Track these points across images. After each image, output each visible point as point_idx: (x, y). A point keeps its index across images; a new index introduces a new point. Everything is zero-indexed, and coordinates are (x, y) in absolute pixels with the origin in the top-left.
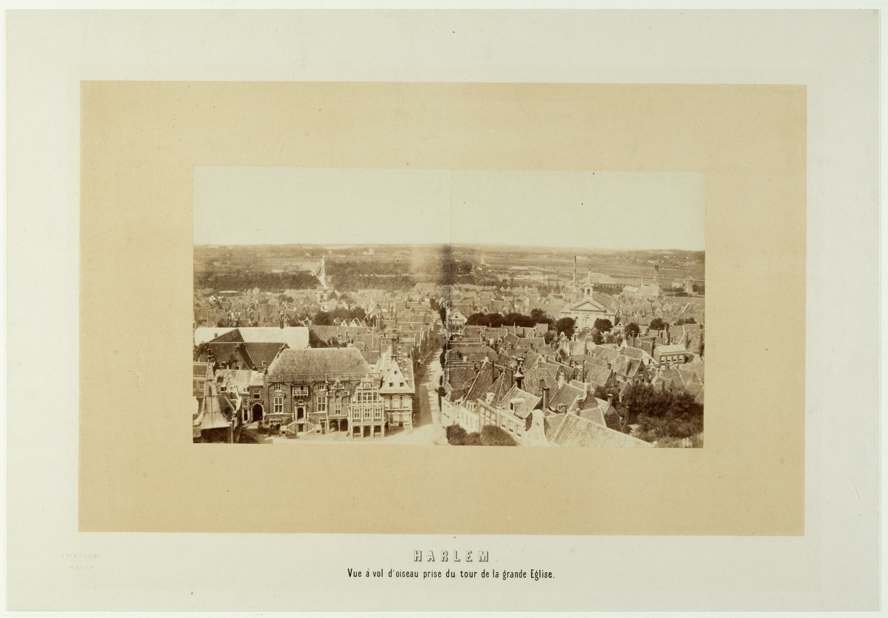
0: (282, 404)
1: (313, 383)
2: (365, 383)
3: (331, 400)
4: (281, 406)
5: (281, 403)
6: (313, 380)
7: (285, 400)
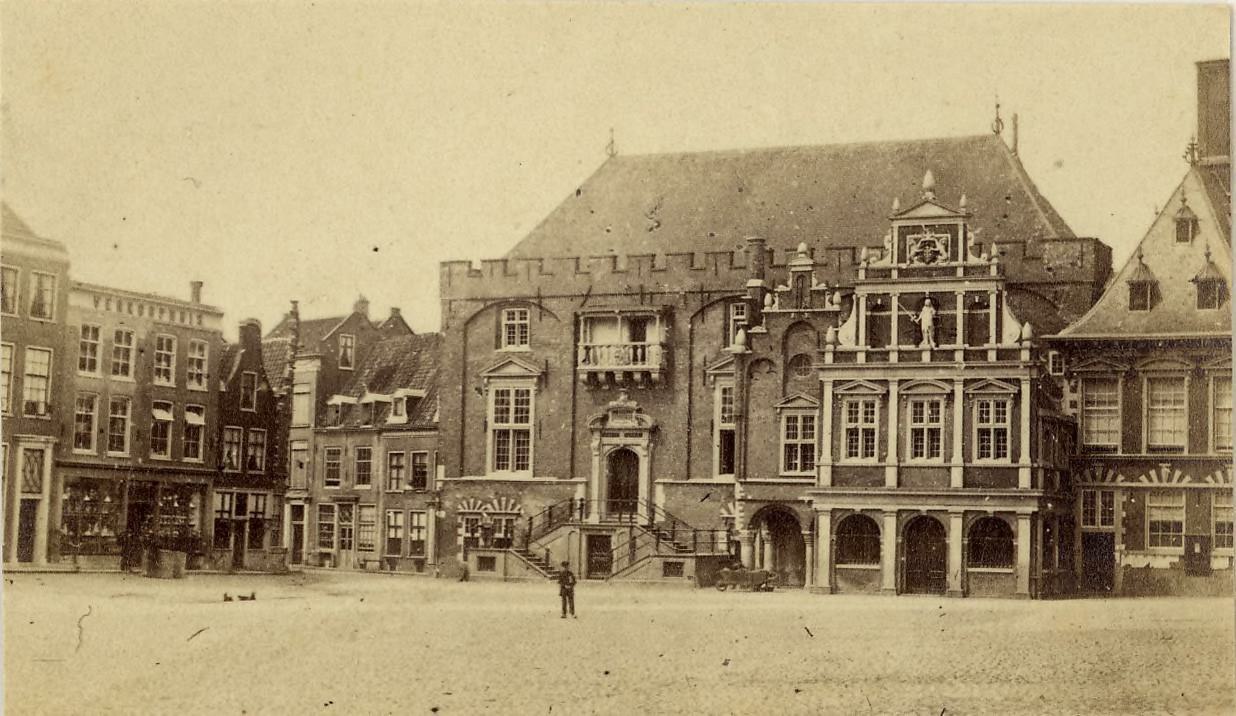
1: (695, 304)
3: (766, 383)
4: (526, 433)
5: (522, 415)
6: (689, 283)
7: (542, 401)
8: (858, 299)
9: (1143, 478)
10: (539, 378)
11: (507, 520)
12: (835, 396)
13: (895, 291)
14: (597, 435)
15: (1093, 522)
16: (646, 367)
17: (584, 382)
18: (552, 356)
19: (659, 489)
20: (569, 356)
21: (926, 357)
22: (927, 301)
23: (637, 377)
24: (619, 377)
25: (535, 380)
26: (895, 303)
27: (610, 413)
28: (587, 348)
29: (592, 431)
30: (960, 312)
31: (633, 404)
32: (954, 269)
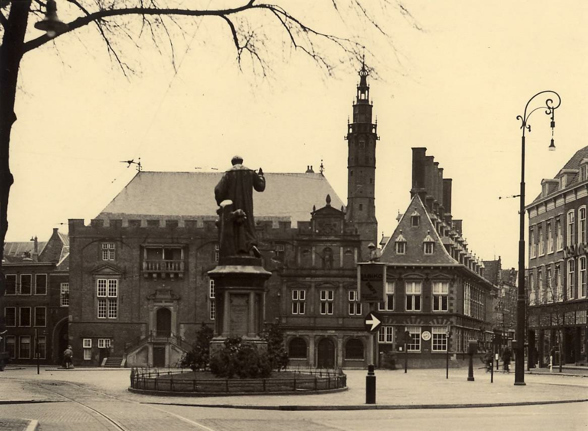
9: (404, 322)
11: (106, 340)
15: (383, 341)
16: (177, 271)
19: (182, 326)
20: (137, 265)
22: (328, 249)
24: (163, 275)
27: (158, 292)
29: (149, 300)
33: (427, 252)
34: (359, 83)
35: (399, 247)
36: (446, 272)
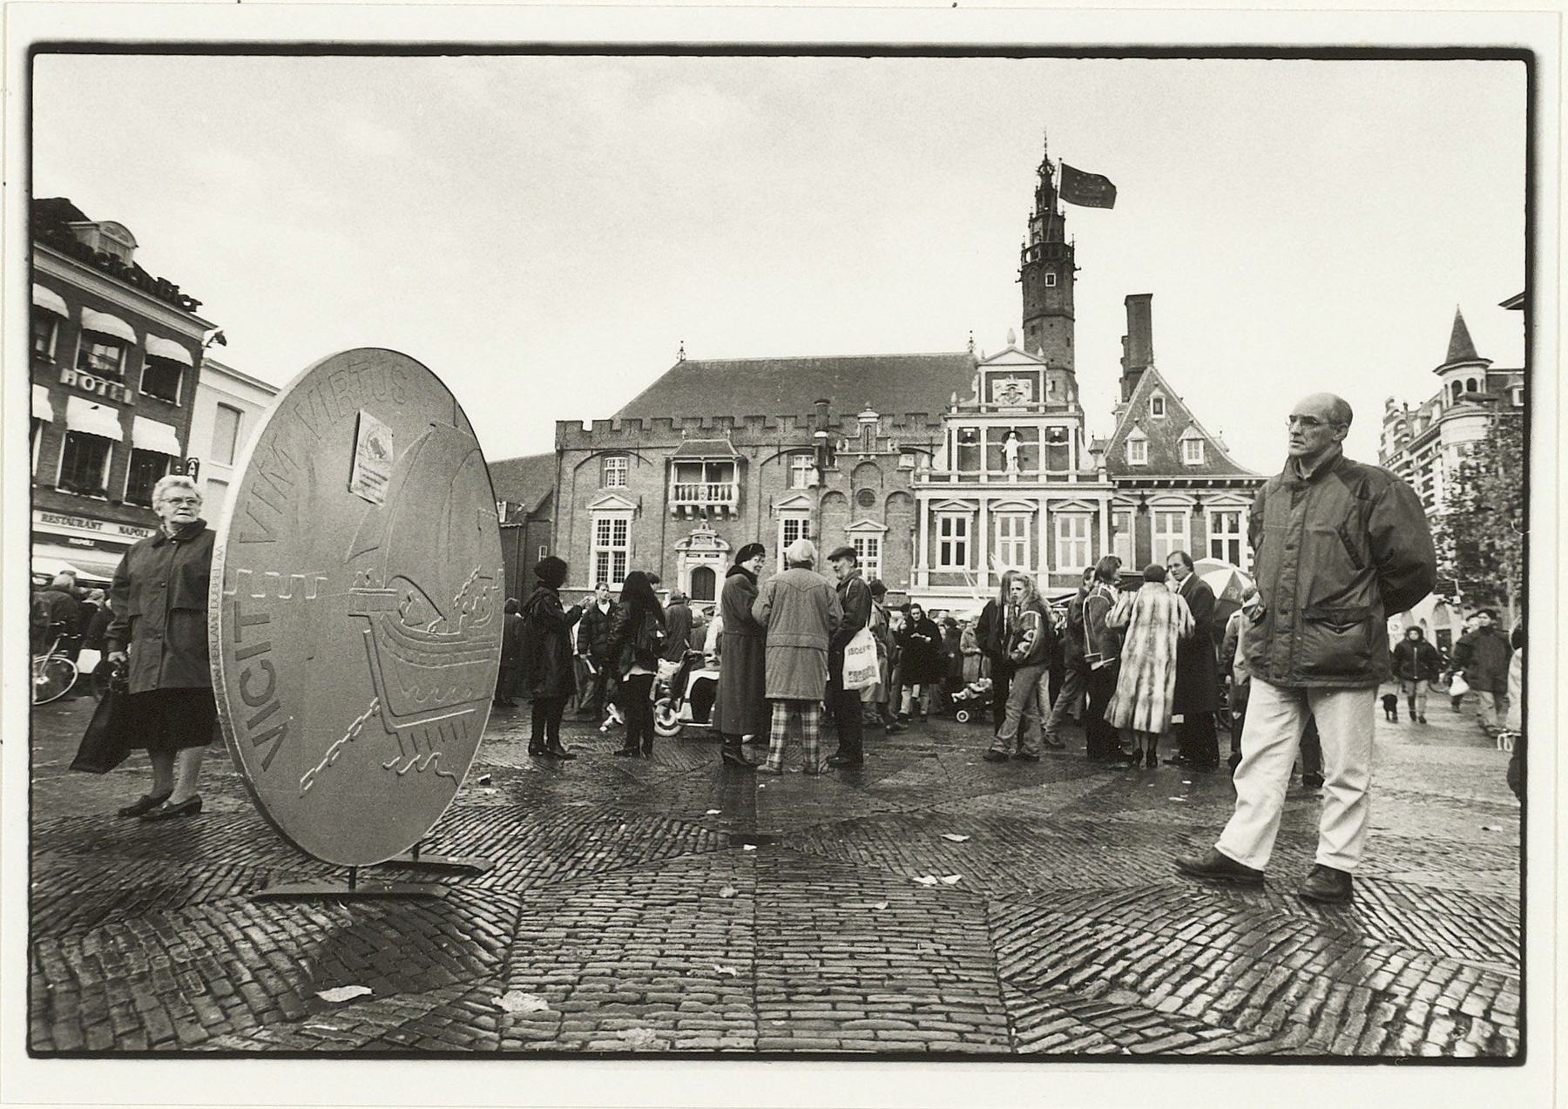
0: (627, 548)
2: (1005, 375)
8: (950, 431)
10: (635, 510)
12: (931, 513)
13: (984, 425)
14: (682, 554)
16: (725, 502)
17: (674, 515)
18: (644, 493)
20: (662, 492)
21: (1013, 481)
22: (1012, 435)
23: (718, 510)
25: (632, 512)
26: (983, 434)
27: (693, 539)
28: (677, 487)
30: (1042, 443)
31: (712, 533)
32: (1037, 409)
33: (1190, 457)
34: (1039, 185)
35: (1134, 448)
36: (1238, 492)
